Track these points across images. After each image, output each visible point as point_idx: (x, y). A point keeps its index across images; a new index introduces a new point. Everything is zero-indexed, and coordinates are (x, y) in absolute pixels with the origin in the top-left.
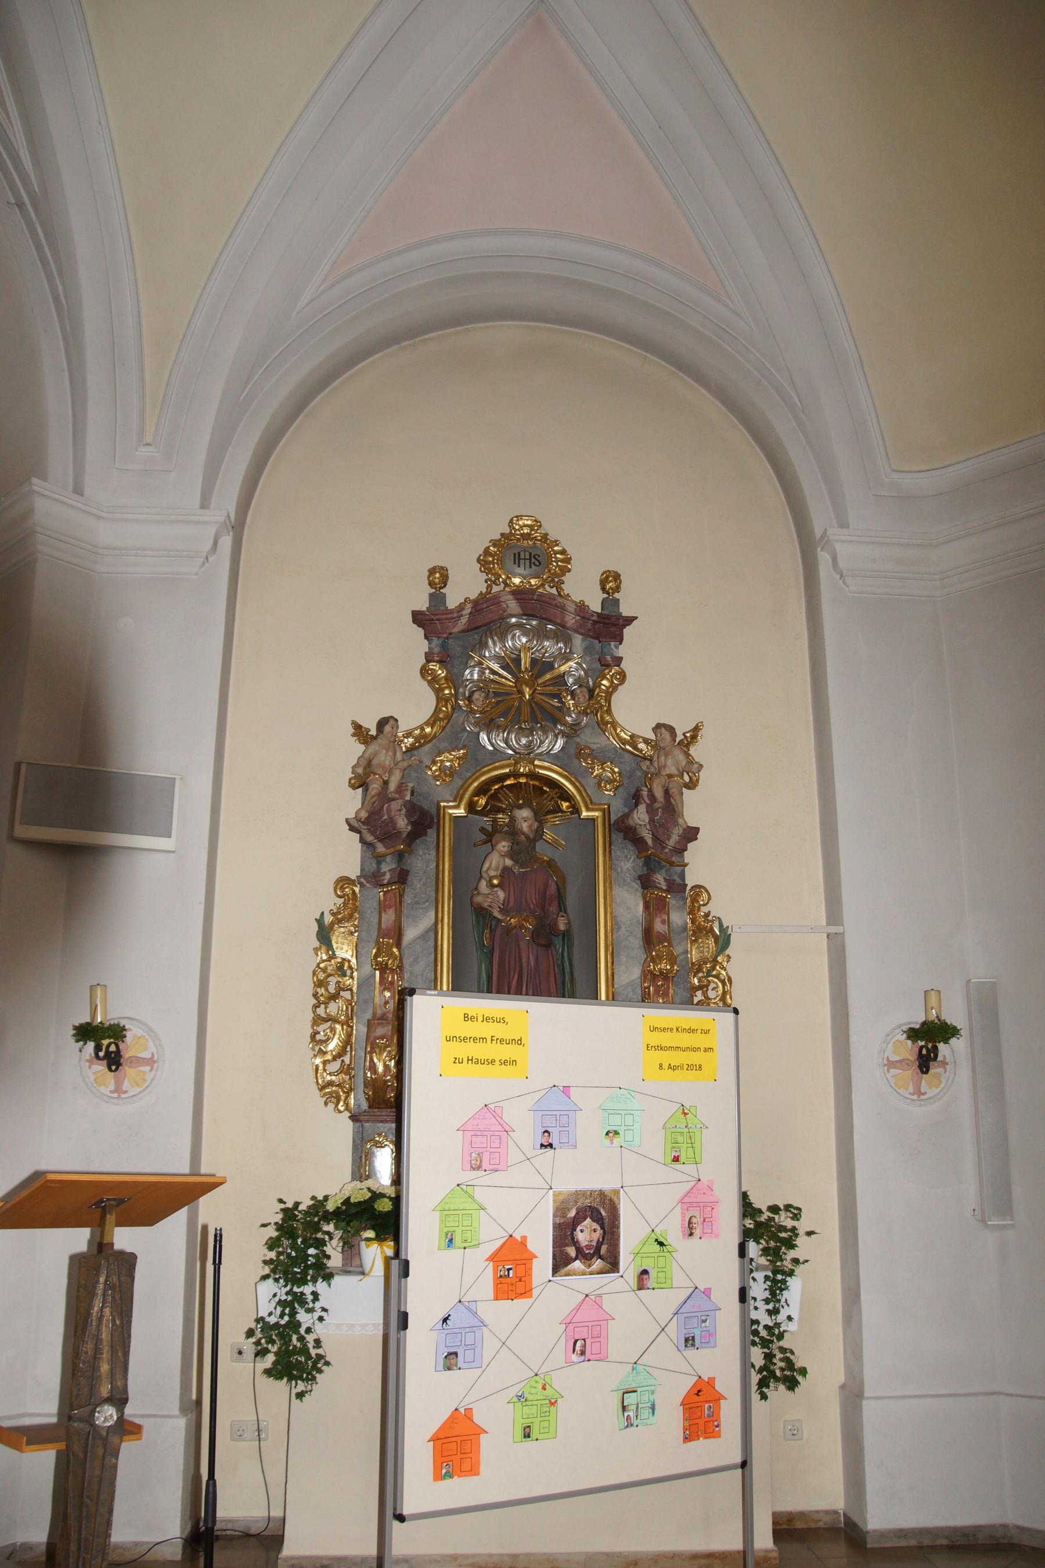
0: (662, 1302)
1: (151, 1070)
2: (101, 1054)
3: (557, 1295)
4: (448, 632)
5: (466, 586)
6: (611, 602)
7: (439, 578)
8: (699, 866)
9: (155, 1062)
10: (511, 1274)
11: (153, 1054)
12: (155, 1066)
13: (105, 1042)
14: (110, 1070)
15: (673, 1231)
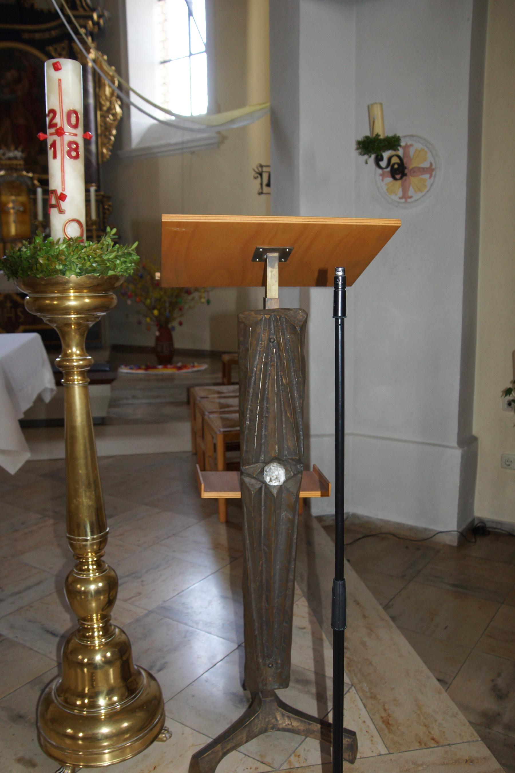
1: (430, 177)
2: (383, 164)
9: (433, 170)
11: (431, 164)
12: (434, 173)
13: (386, 155)
14: (395, 179)
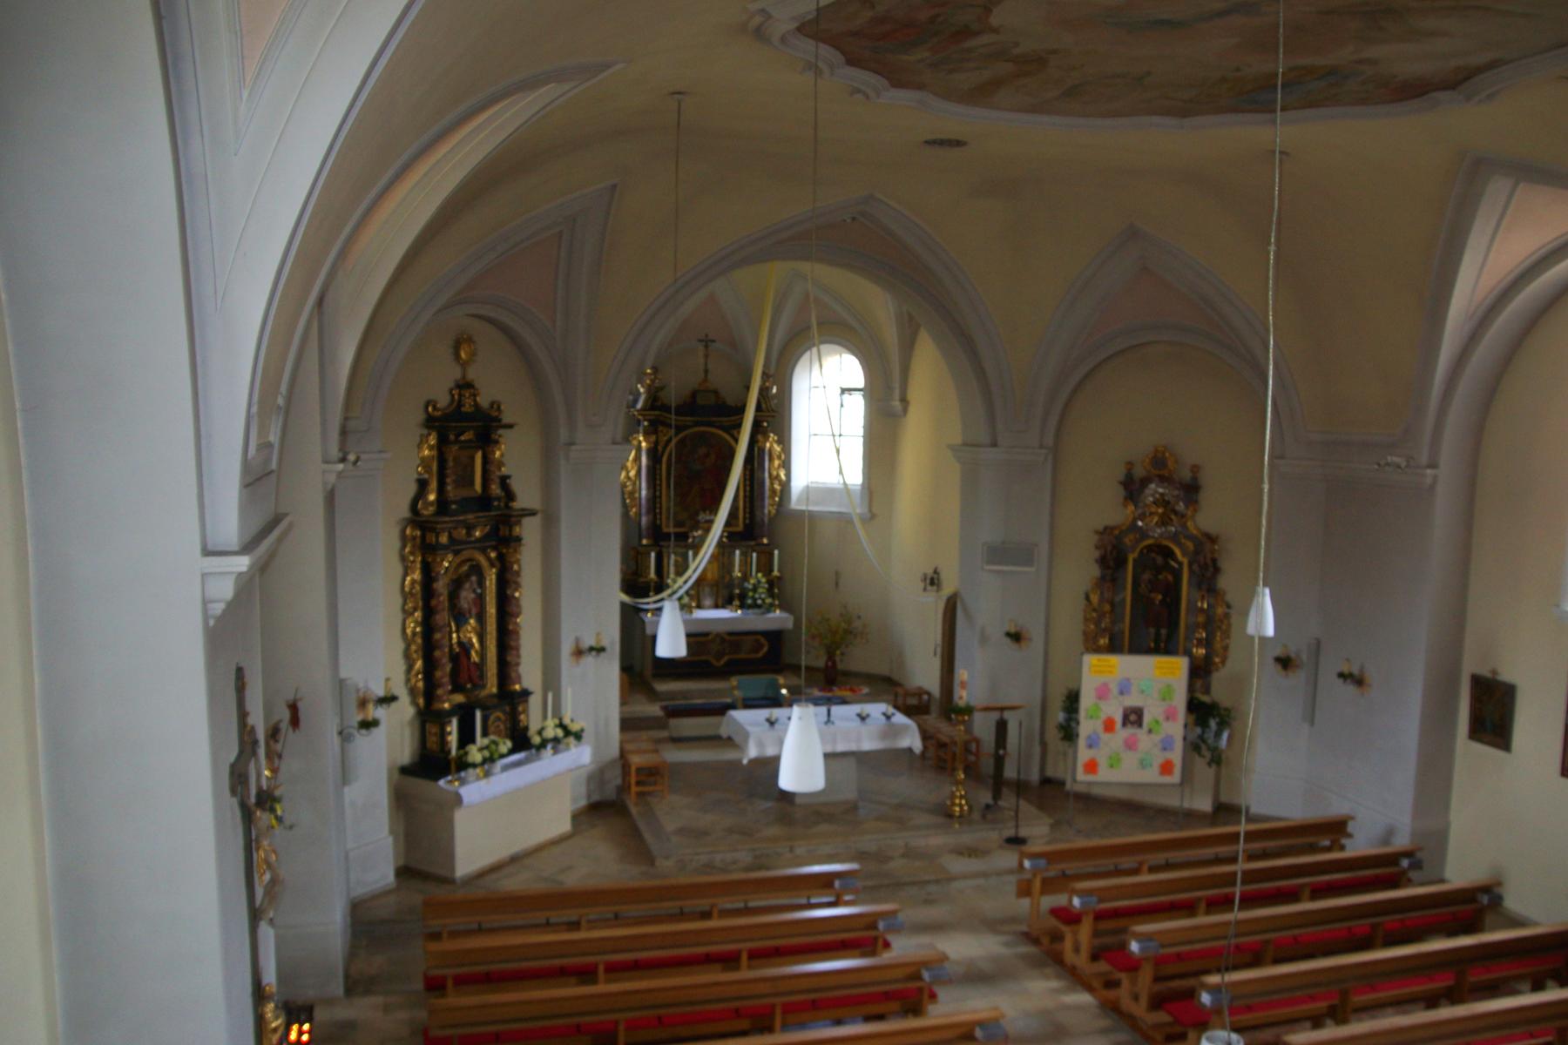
0: (1156, 738)
3: (1122, 734)
4: (1132, 488)
5: (1139, 472)
6: (1195, 479)
7: (1130, 465)
8: (1223, 582)
10: (1109, 726)
15: (1161, 718)
